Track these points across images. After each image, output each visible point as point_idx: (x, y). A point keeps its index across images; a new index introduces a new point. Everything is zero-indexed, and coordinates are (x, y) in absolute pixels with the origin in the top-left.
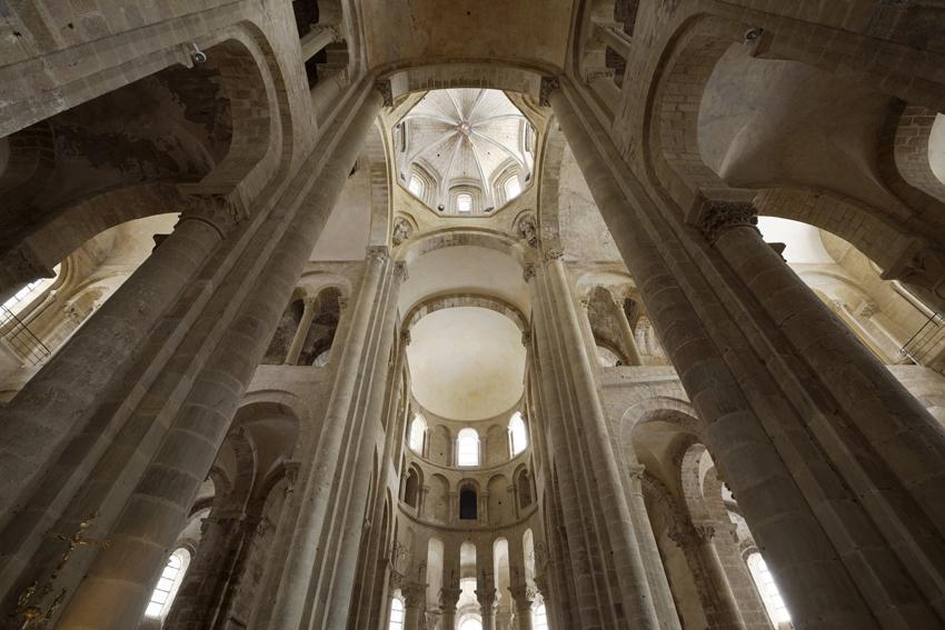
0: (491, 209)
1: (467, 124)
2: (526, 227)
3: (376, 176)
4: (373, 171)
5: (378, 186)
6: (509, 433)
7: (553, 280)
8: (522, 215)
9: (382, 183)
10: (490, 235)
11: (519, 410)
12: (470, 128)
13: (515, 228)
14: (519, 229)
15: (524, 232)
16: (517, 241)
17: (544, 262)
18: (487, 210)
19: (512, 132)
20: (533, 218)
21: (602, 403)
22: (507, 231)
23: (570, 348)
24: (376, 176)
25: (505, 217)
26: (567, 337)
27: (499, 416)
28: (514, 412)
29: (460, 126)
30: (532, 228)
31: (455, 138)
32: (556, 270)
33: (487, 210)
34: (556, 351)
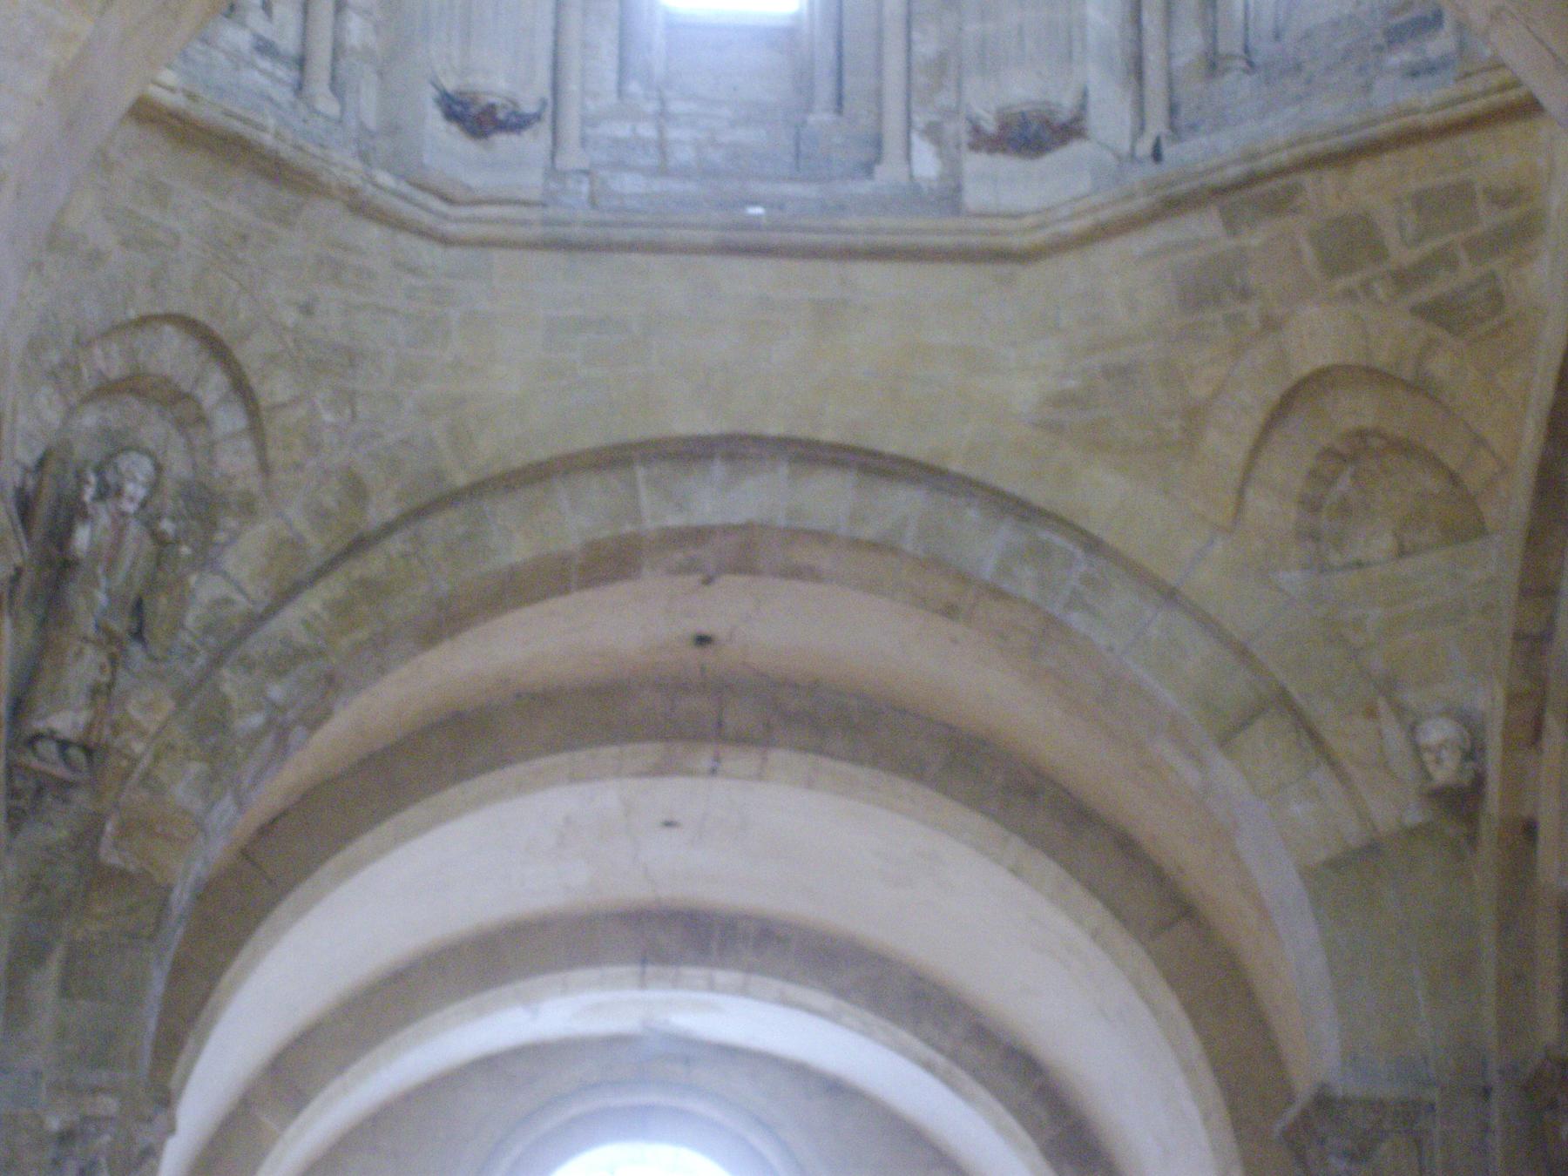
8: (171, 354)
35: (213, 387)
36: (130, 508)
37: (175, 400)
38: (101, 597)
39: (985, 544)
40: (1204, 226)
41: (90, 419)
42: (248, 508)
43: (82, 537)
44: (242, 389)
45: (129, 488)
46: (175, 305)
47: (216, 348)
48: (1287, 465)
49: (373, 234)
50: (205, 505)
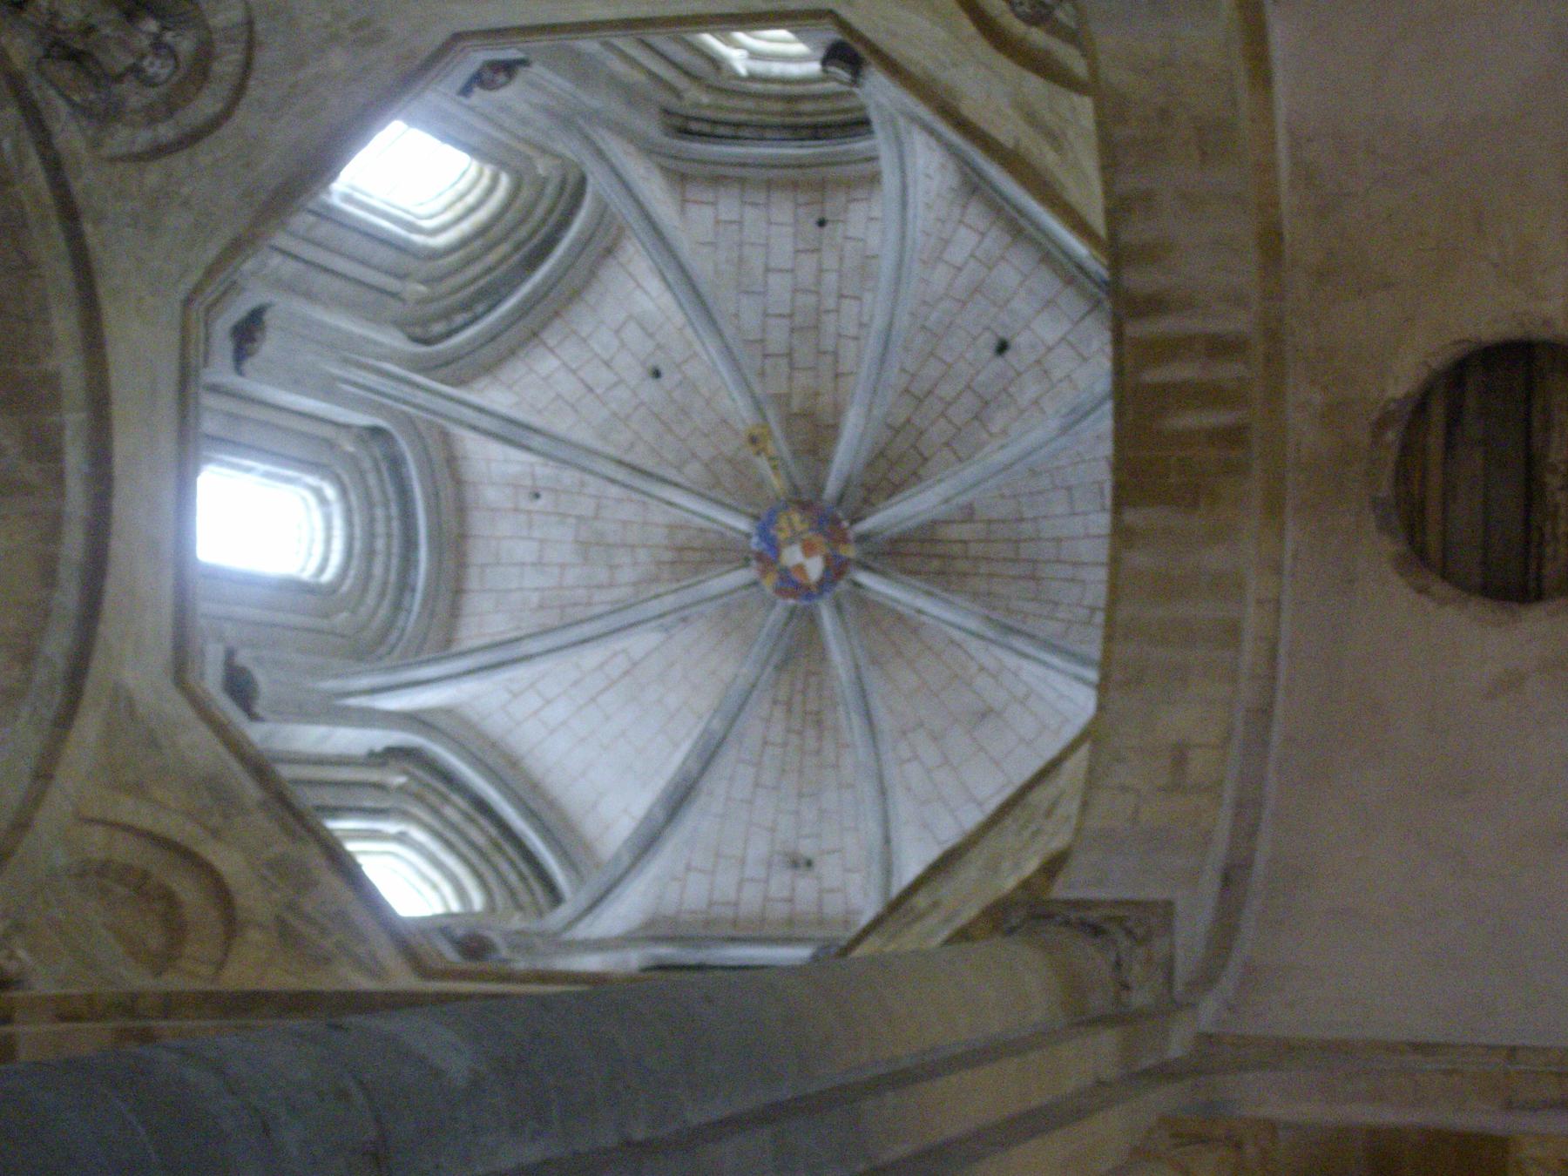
1: (791, 584)
3: (1210, 395)
4: (1234, 436)
5: (1194, 324)
8: (206, 105)
9: (1171, 349)
12: (768, 557)
18: (508, 68)
19: (504, 527)
24: (1210, 395)
29: (836, 569)
31: (889, 471)
35: (166, 131)
36: (146, 63)
37: (170, 108)
38: (107, 31)
39: (57, 645)
40: (251, 791)
41: (185, 45)
42: (95, 144)
43: (152, 26)
44: (159, 151)
45: (158, 63)
46: (241, 116)
47: (193, 137)
48: (126, 851)
49: (211, 253)
50: (105, 115)
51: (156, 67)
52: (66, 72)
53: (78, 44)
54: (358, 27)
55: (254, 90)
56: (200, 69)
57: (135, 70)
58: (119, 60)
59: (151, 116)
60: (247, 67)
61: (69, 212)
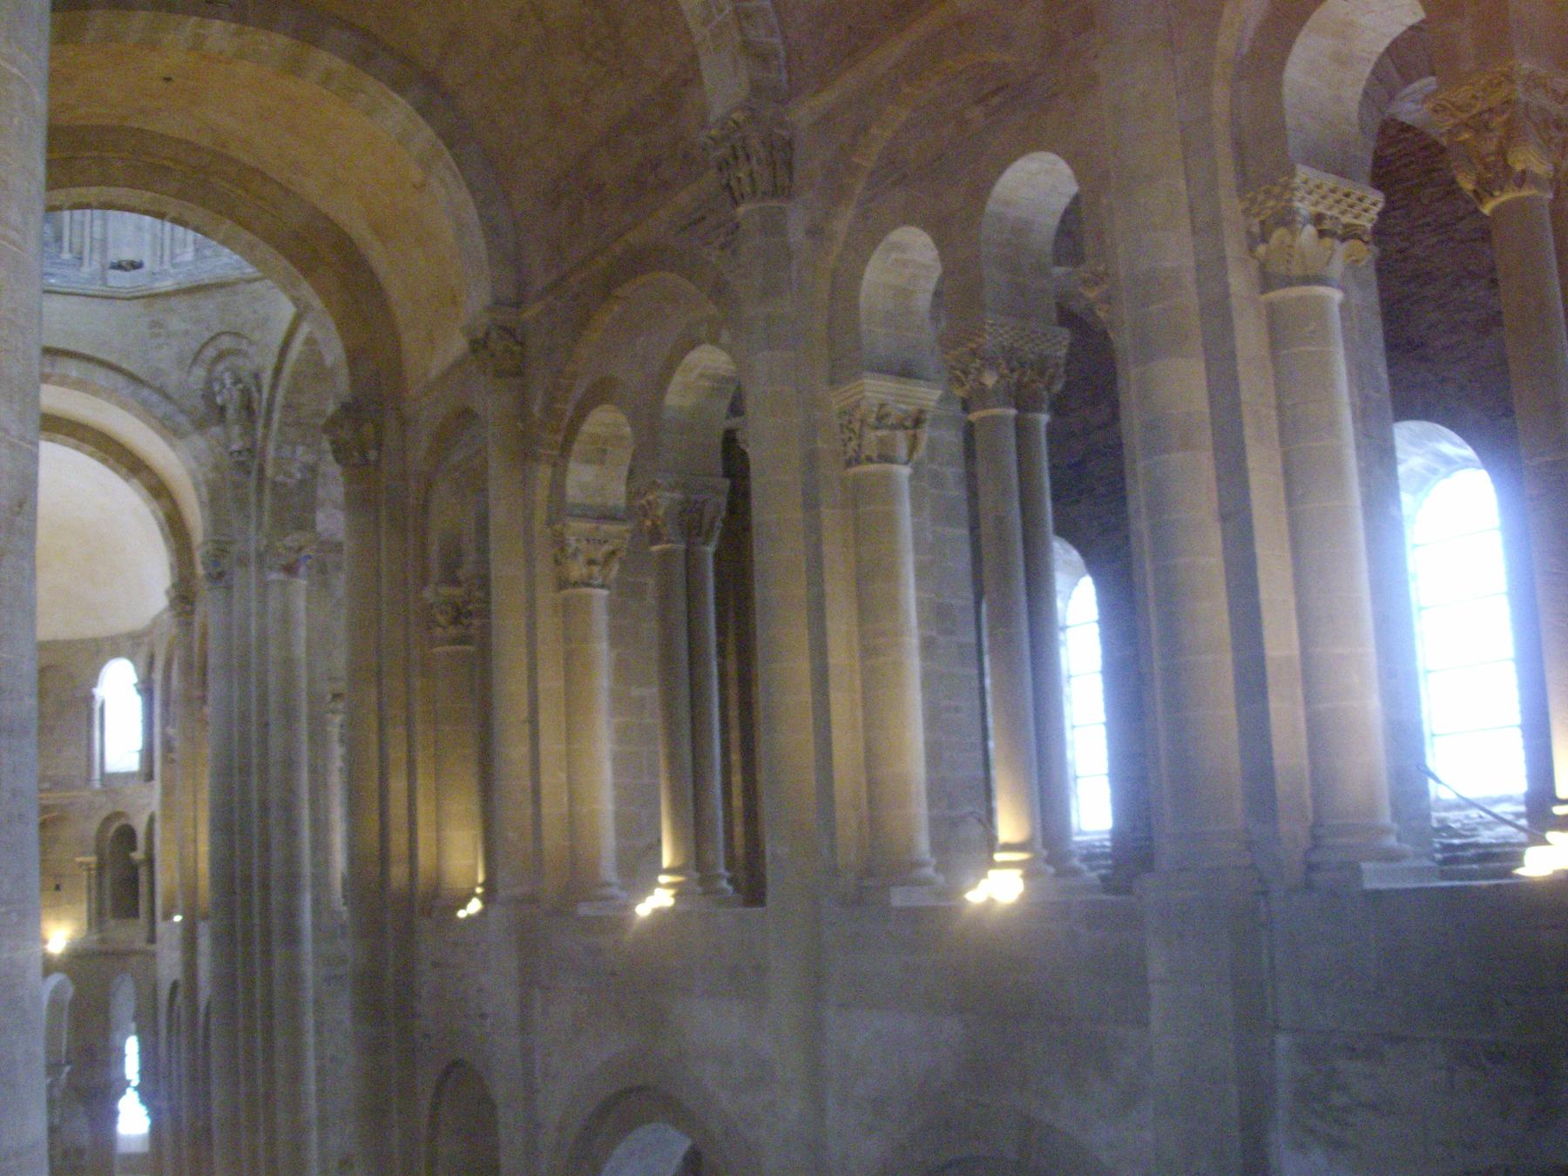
0: (136, 266)
2: (228, 396)
6: (97, 707)
7: (273, 651)
8: (226, 343)
10: (120, 381)
11: (131, 658)
13: (200, 373)
14: (209, 382)
15: (222, 409)
16: (200, 425)
17: (260, 556)
18: (119, 266)
20: (257, 376)
21: (318, 1032)
22: (173, 379)
23: (276, 899)
25: (176, 324)
26: (277, 856)
27: (69, 644)
28: (116, 654)
30: (248, 408)
32: (286, 618)
33: (119, 266)
34: (247, 881)
37: (237, 352)
43: (219, 400)
46: (216, 331)
51: (228, 382)
52: (255, 406)
53: (244, 414)
54: (158, 336)
55: (207, 335)
56: (221, 356)
57: (235, 384)
58: (236, 394)
59: (245, 354)
60: (205, 345)
61: (278, 371)
